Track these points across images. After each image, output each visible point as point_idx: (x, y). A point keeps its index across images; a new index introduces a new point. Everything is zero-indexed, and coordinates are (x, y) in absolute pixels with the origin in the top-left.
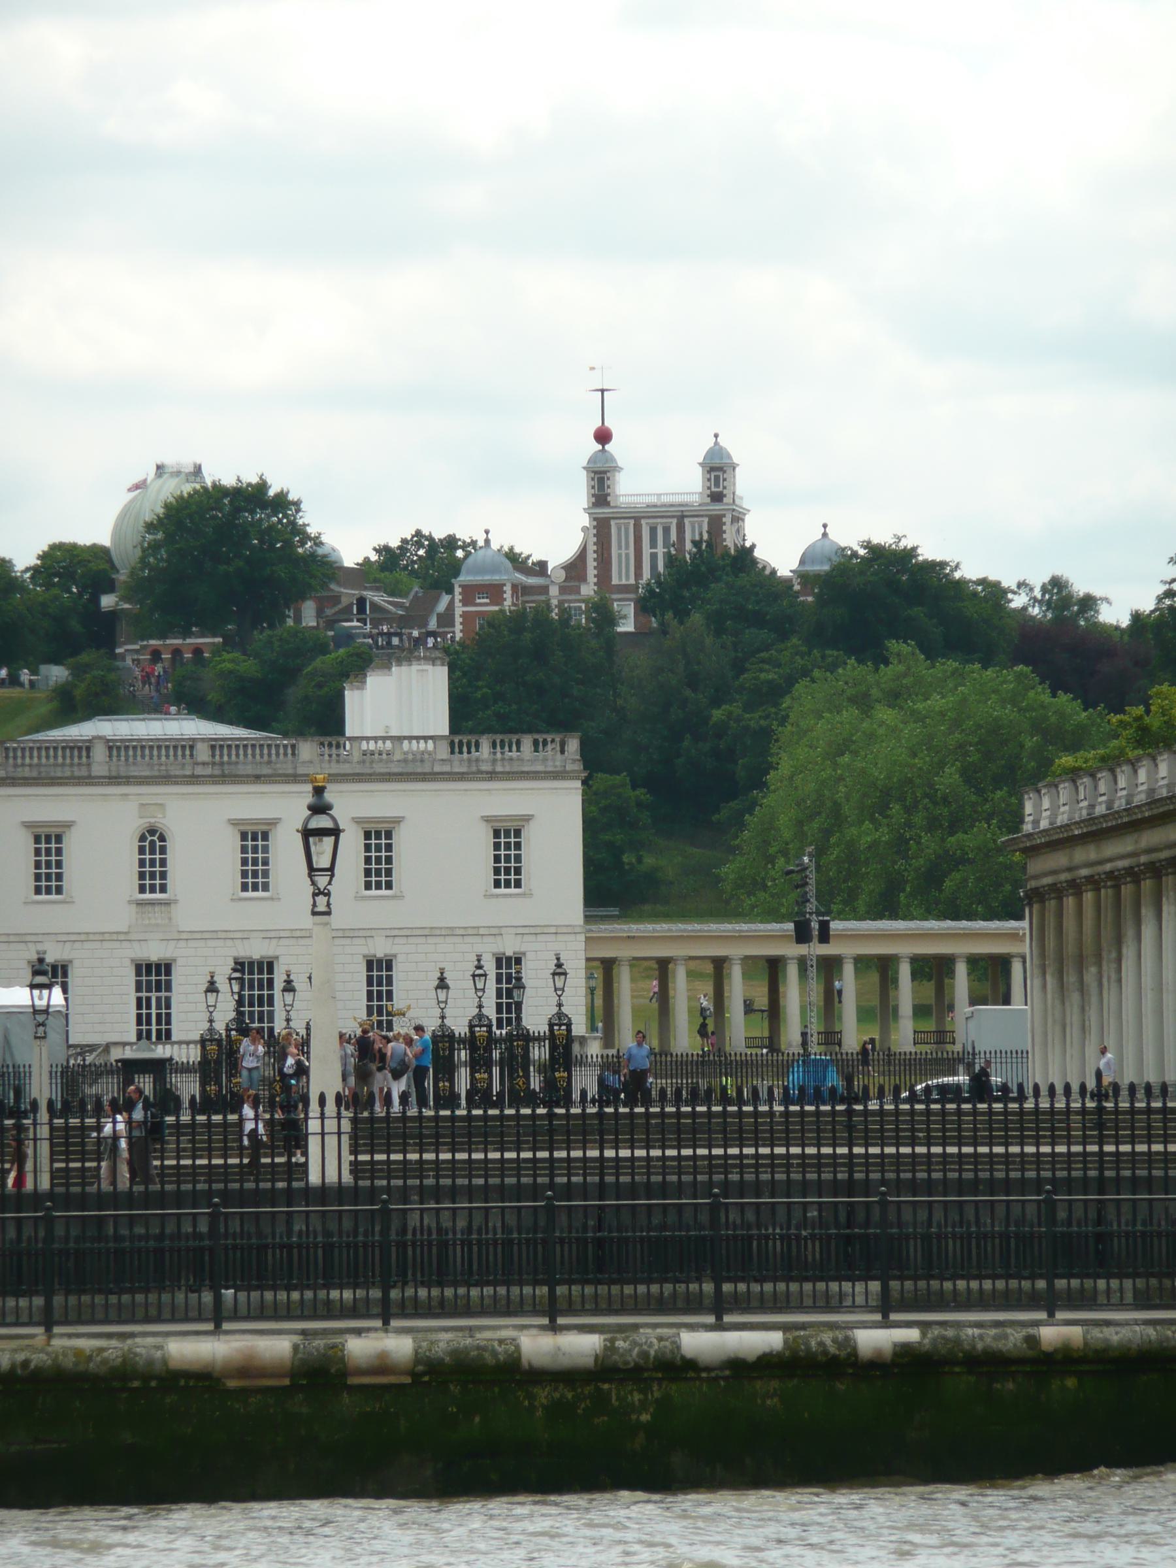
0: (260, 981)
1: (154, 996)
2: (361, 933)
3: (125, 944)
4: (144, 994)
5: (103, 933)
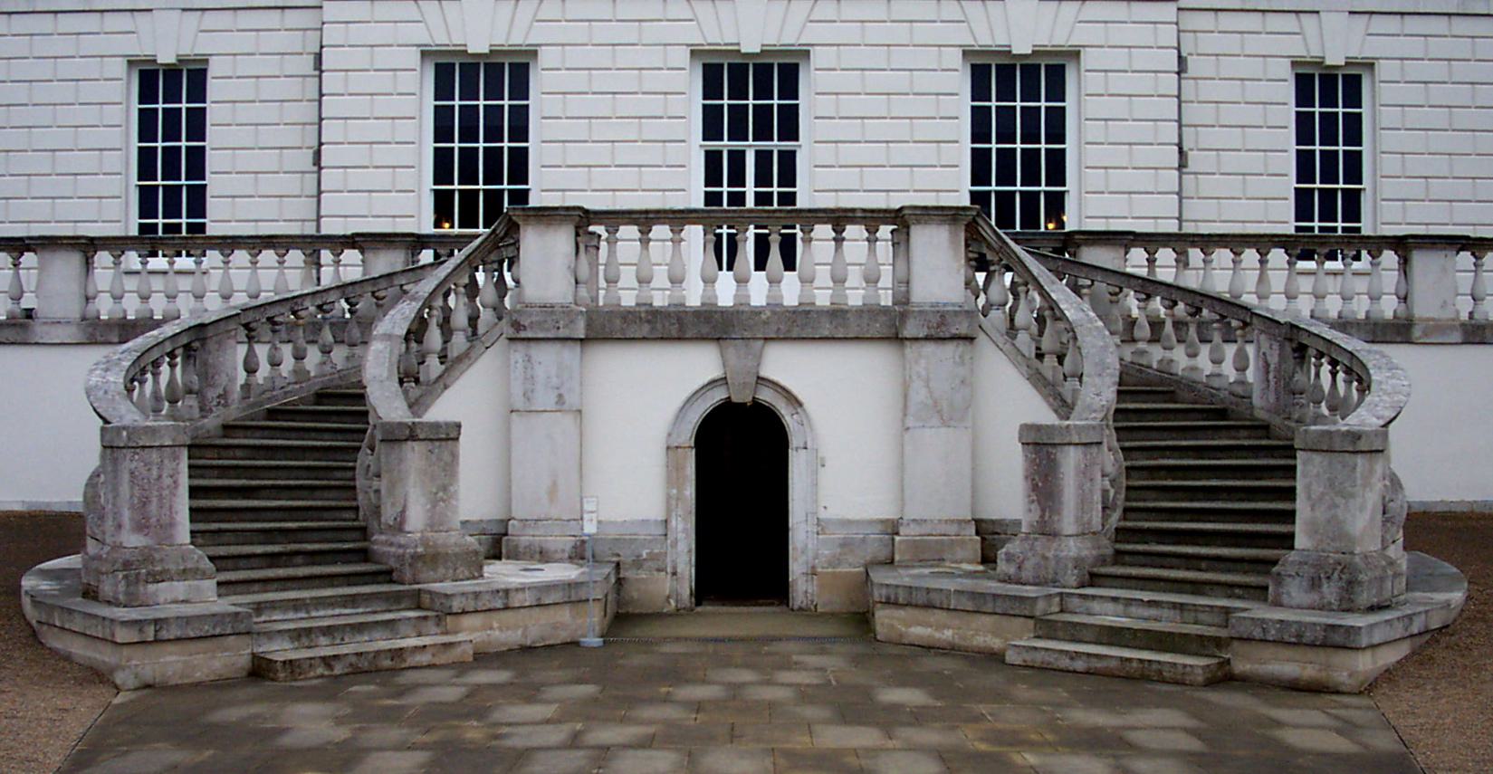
0: (1031, 115)
1: (750, 148)
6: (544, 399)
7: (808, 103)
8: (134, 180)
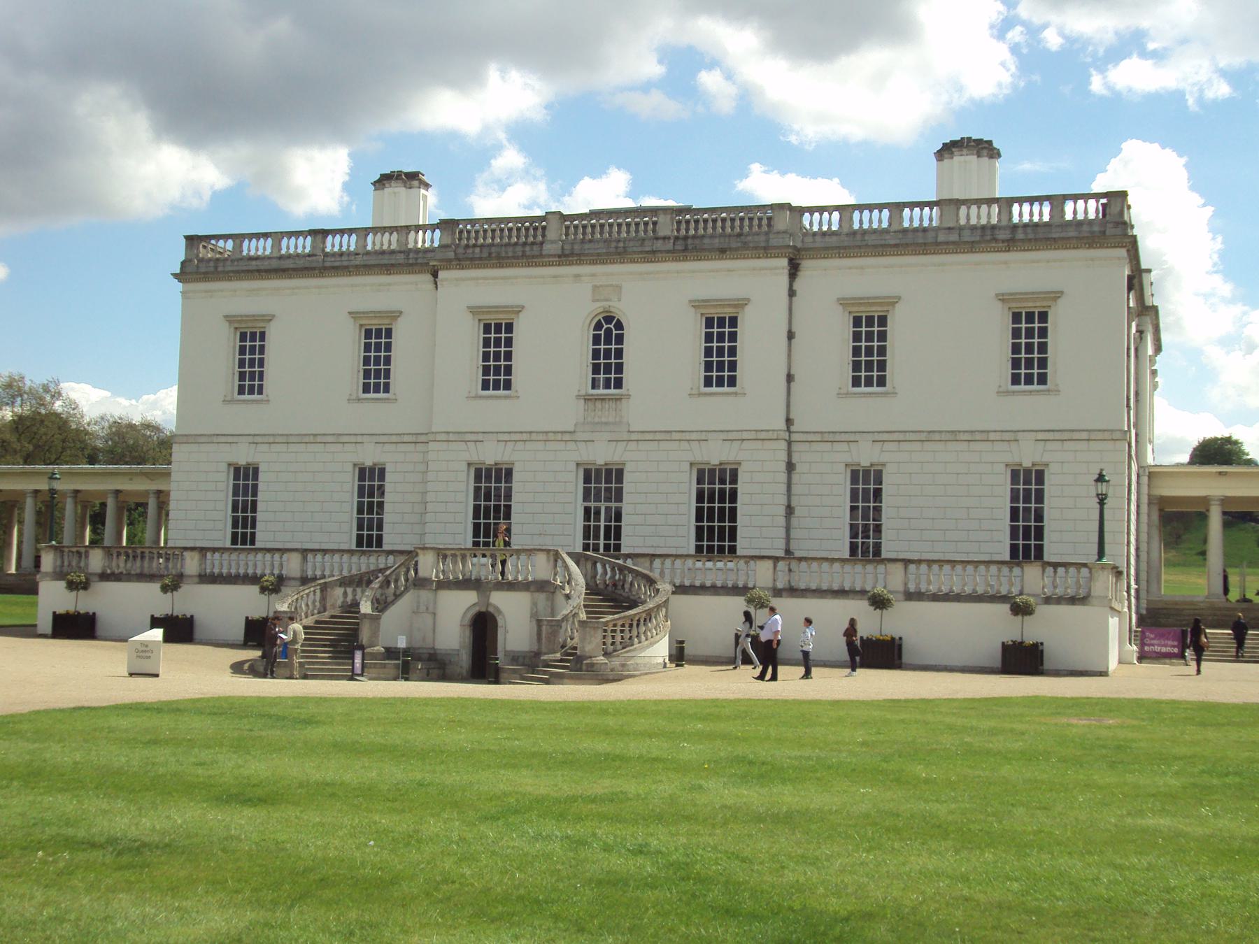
1: (603, 506)
2: (844, 437)
3: (571, 446)
4: (592, 504)
5: (547, 433)
6: (423, 608)
7: (627, 487)
8: (355, 515)
